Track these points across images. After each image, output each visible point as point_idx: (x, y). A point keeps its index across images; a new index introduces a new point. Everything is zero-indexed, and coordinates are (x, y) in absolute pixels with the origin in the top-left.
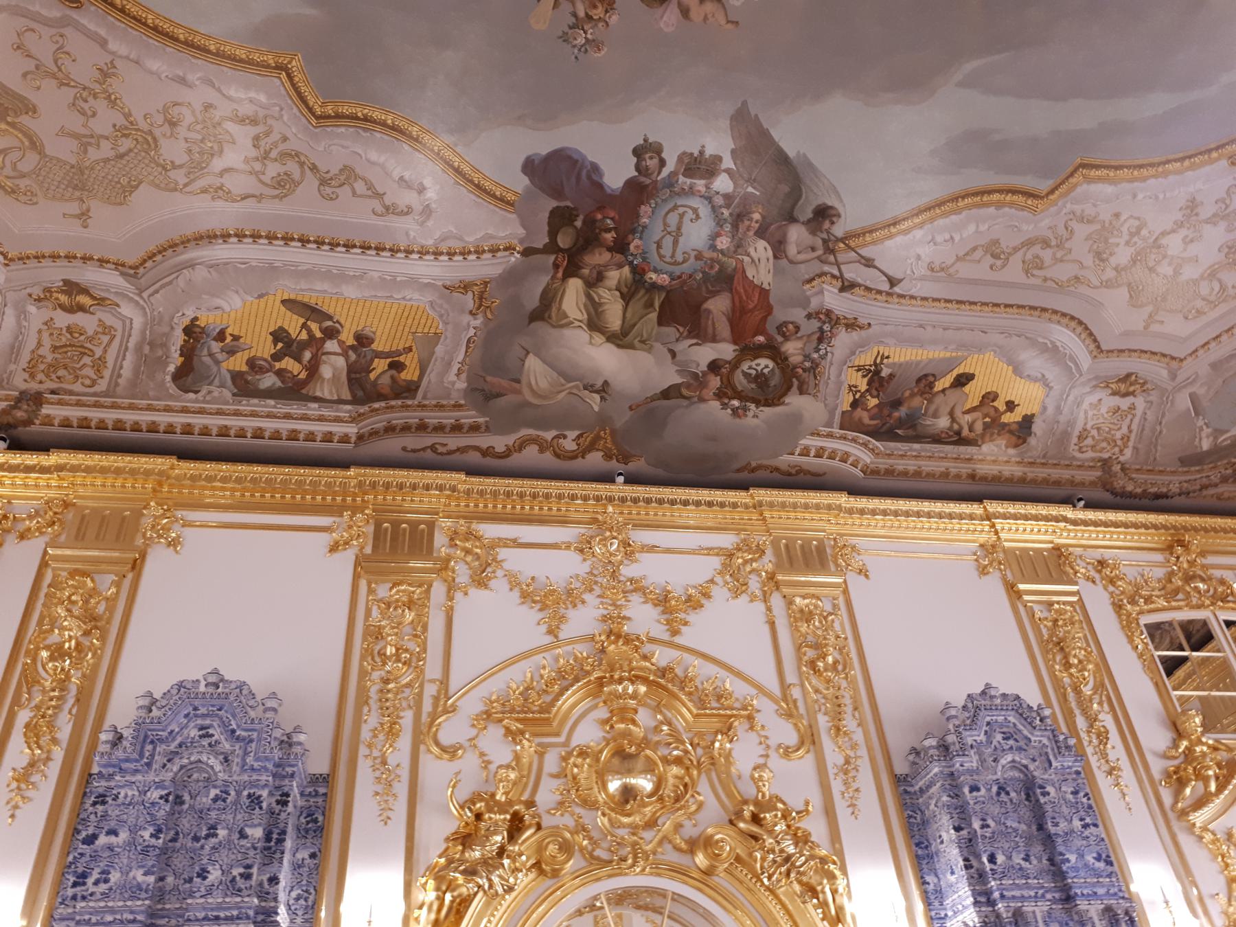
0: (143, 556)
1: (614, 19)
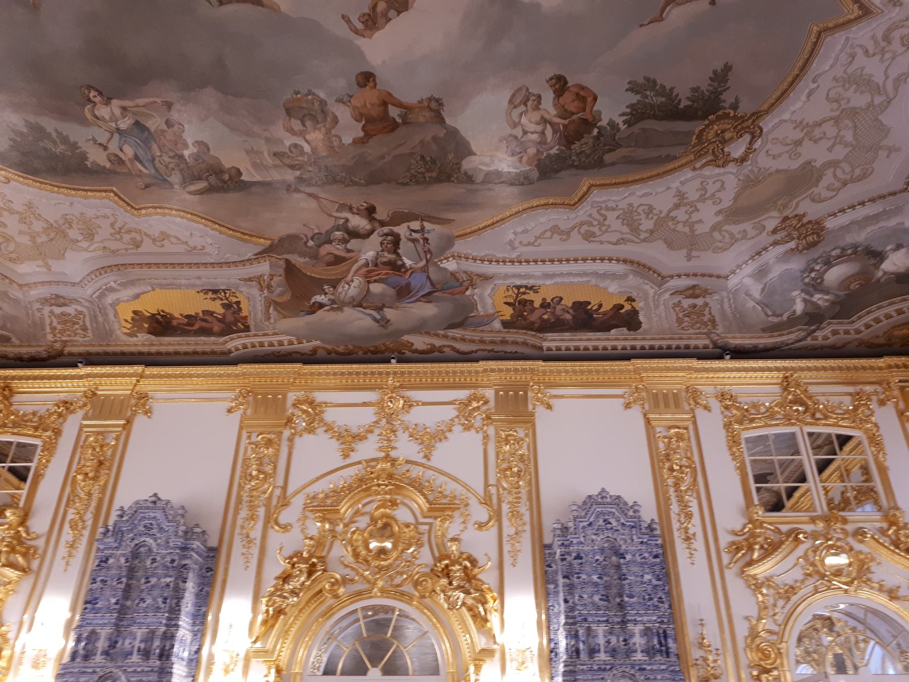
0: (129, 422)
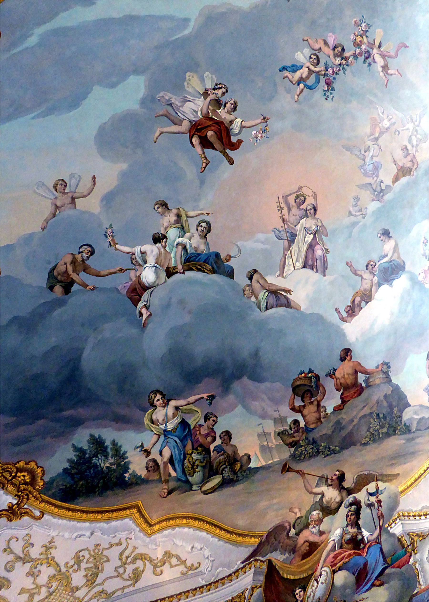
1: (352, 37)
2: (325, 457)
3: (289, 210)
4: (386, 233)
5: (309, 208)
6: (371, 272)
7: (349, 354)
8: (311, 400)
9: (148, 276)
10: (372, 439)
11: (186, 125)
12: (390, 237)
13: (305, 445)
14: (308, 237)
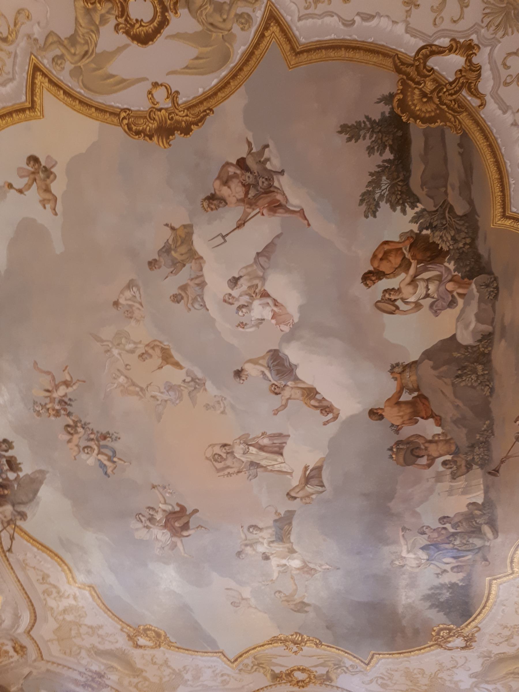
1: (53, 418)
2: (493, 435)
3: (228, 467)
4: (238, 374)
5: (224, 450)
6: (283, 389)
7: (375, 411)
8: (422, 449)
9: (295, 563)
10: (488, 383)
11: (175, 539)
12: (242, 370)
13: (473, 455)
14: (252, 451)
